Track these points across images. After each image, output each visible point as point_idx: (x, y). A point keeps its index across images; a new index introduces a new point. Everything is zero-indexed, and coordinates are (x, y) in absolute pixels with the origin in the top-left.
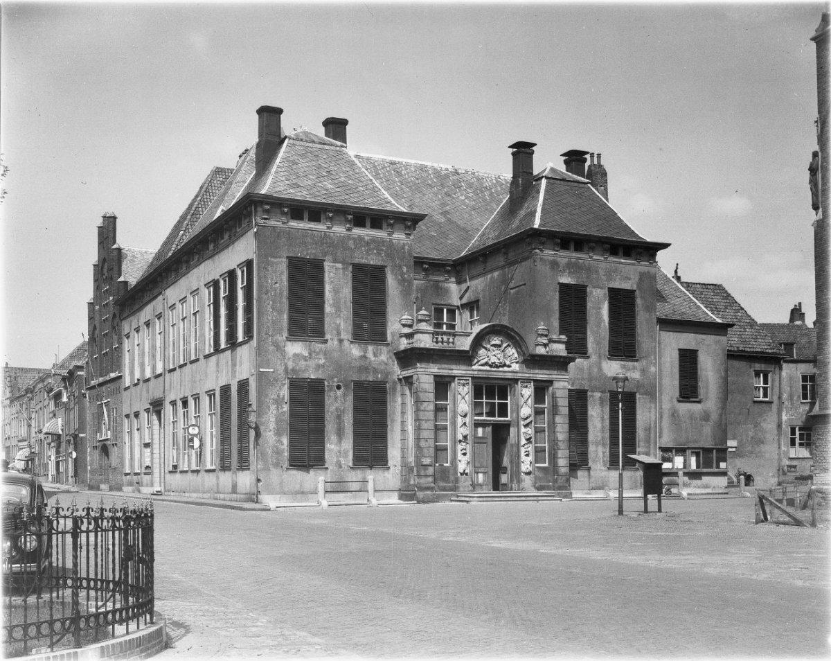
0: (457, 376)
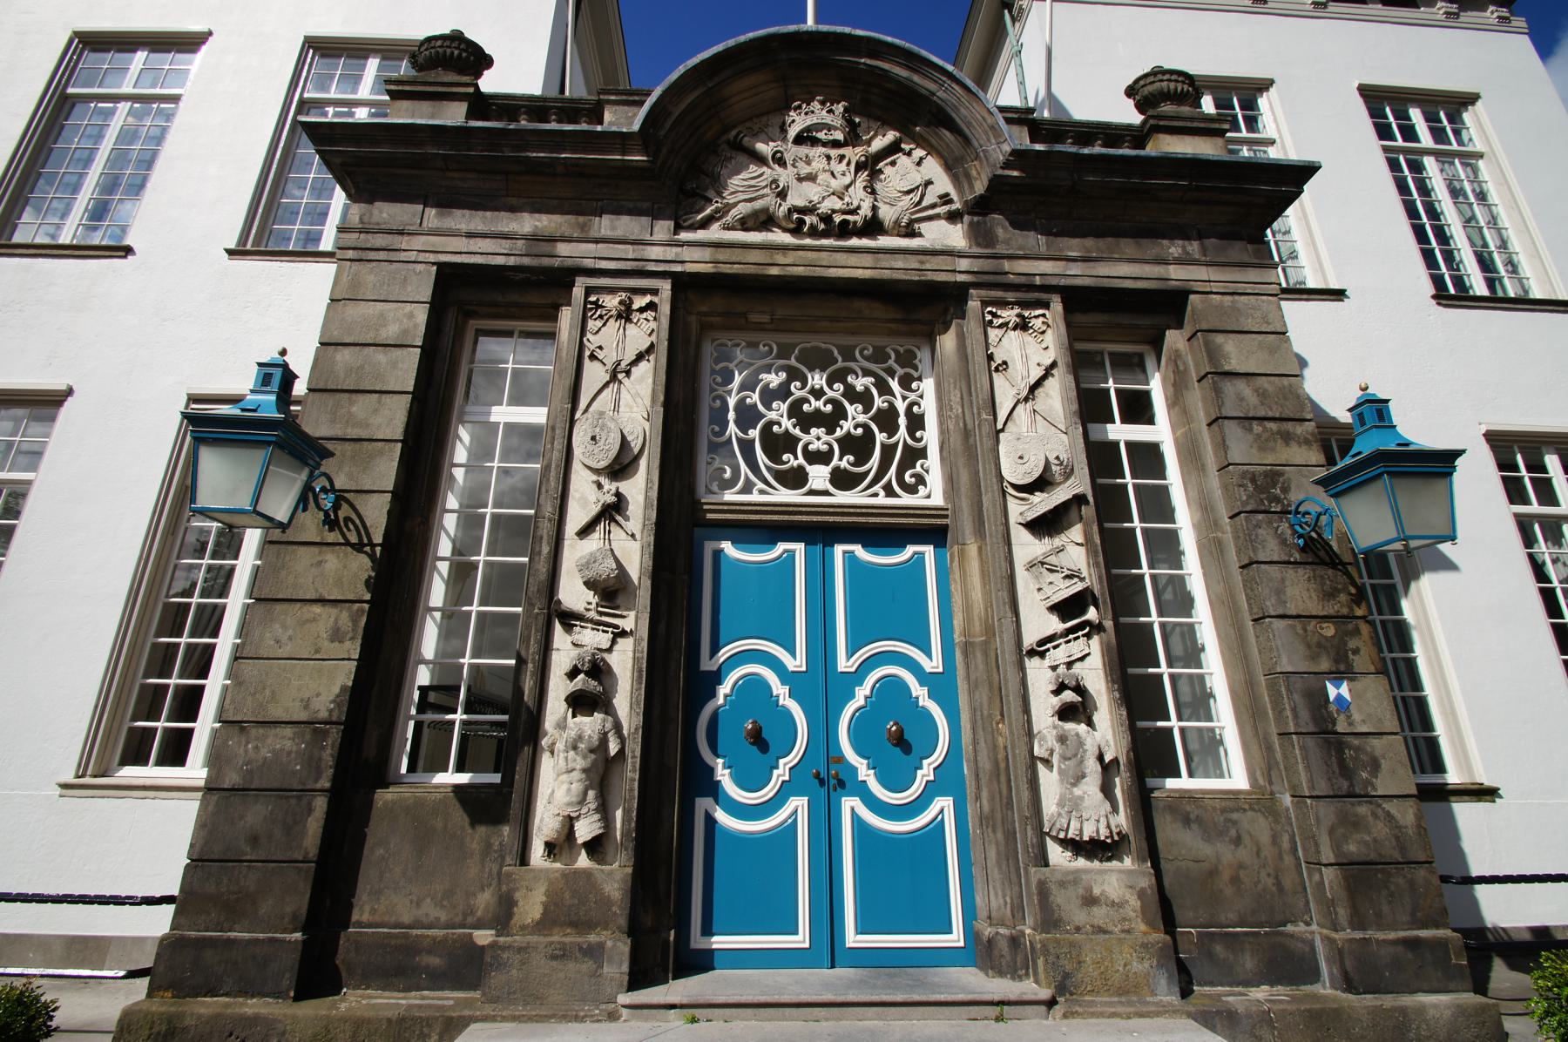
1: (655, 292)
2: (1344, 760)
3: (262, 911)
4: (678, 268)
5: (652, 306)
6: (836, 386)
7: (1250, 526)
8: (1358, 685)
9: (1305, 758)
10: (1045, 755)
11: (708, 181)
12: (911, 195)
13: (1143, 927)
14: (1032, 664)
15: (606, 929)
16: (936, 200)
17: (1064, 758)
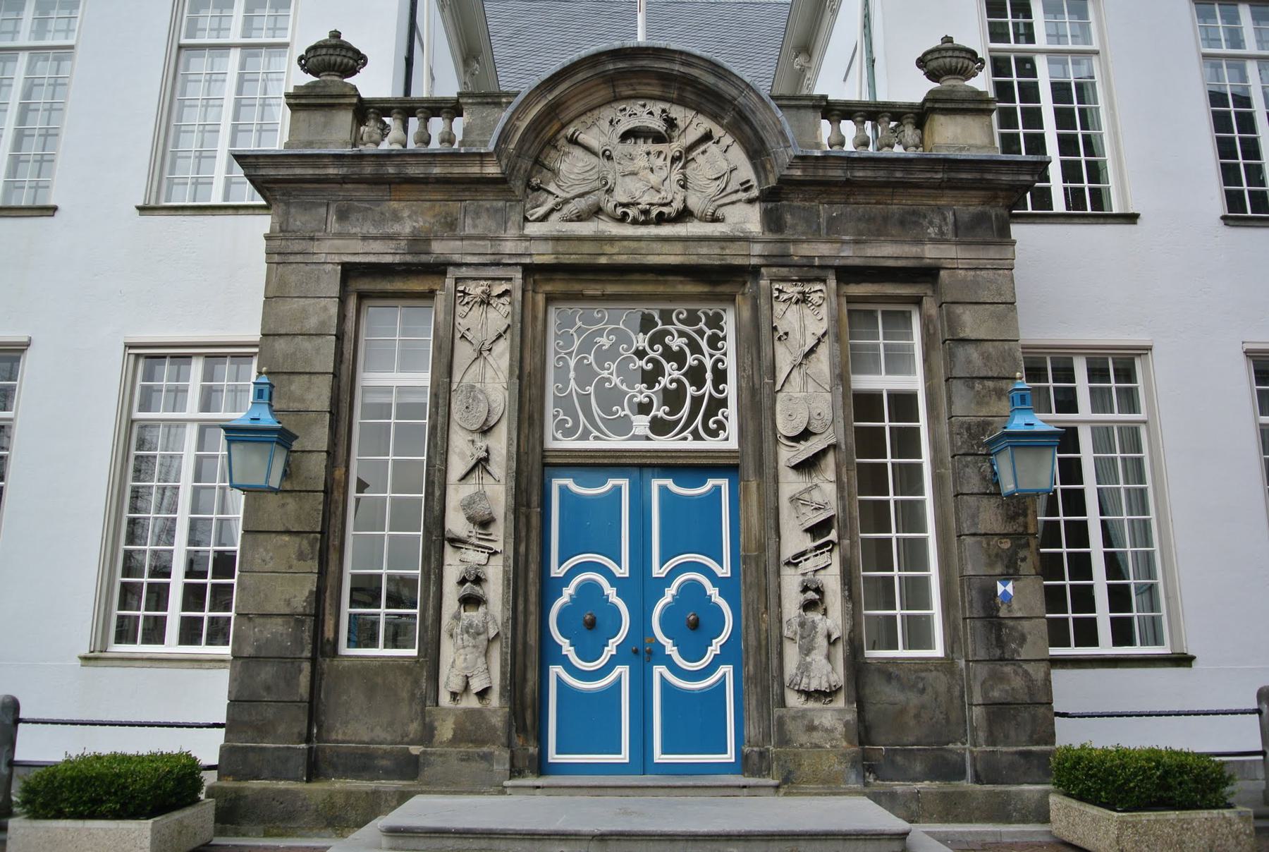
0: (459, 265)
1: (510, 279)
2: (1001, 636)
3: (279, 732)
4: (527, 260)
5: (506, 293)
6: (656, 347)
7: (960, 466)
8: (1020, 584)
9: (973, 635)
10: (791, 635)
11: (550, 174)
12: (718, 182)
13: (845, 744)
14: (787, 572)
15: (494, 744)
16: (738, 187)
17: (802, 637)
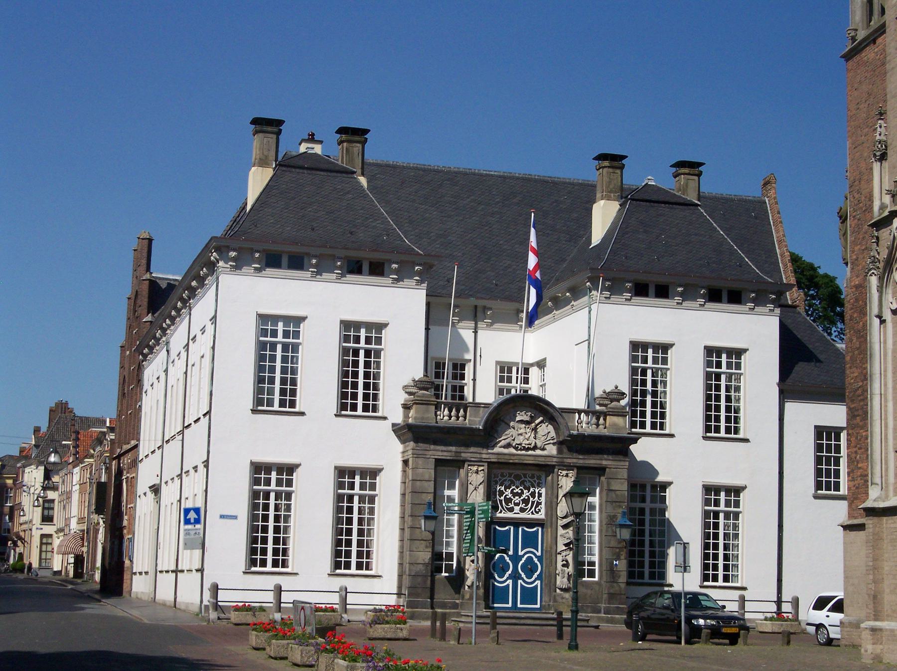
1: (483, 466)
4: (489, 460)
5: (483, 470)
